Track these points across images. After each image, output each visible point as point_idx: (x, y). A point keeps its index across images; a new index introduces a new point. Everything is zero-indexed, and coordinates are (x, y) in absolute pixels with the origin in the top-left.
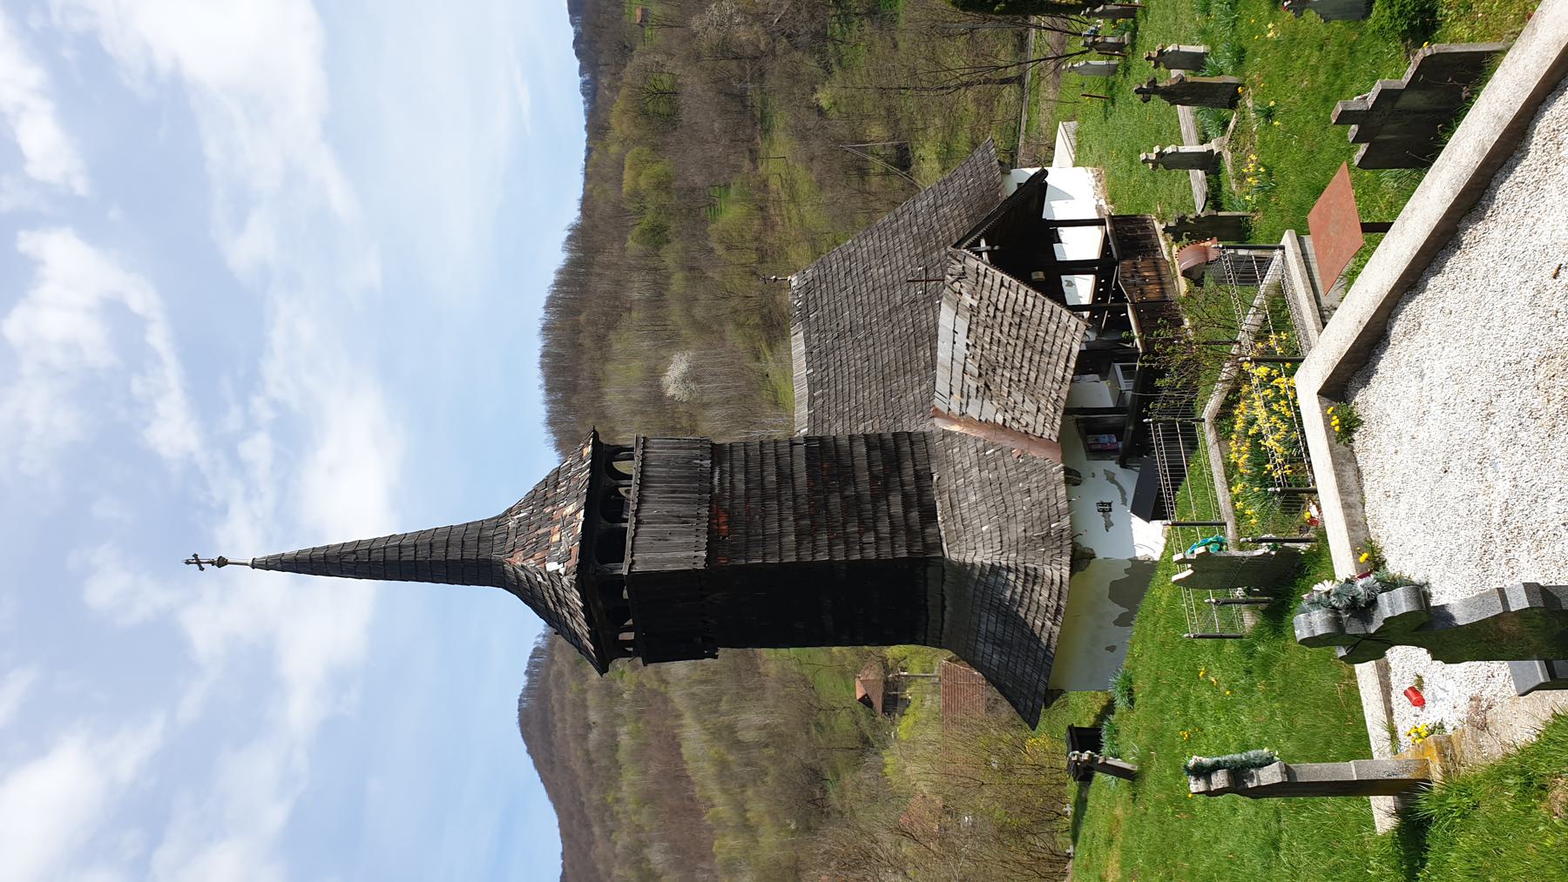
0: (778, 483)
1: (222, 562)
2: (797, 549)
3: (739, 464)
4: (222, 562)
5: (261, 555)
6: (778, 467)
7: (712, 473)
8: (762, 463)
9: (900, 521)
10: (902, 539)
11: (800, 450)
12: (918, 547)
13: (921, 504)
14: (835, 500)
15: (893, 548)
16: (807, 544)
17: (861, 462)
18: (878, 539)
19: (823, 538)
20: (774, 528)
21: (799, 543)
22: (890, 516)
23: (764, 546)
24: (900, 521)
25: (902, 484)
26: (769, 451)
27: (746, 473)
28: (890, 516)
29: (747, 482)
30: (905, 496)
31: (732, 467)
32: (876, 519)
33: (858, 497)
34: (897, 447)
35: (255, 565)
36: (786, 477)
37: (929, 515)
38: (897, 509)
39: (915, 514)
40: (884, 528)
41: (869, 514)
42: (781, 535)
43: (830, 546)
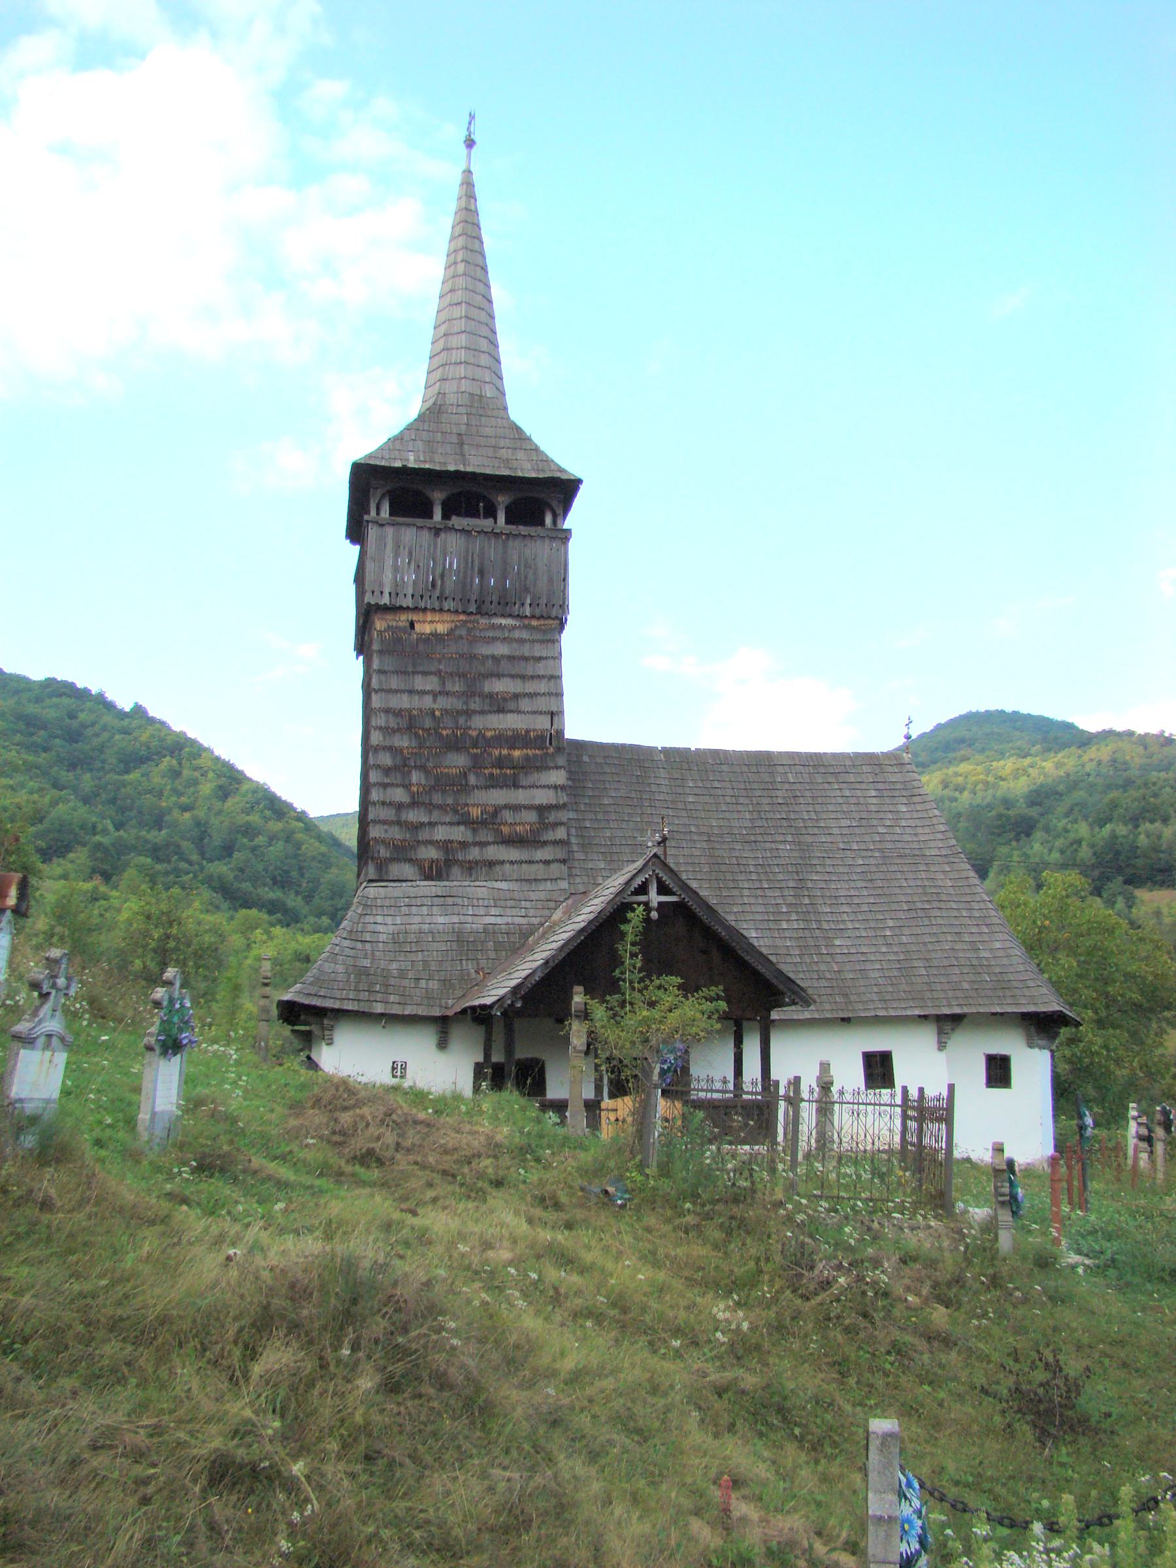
0: (491, 696)
1: (470, 143)
2: (387, 711)
3: (526, 650)
4: (470, 143)
5: (476, 178)
6: (516, 696)
7: (510, 616)
8: (523, 677)
9: (424, 835)
10: (396, 833)
11: (542, 723)
12: (384, 852)
13: (449, 863)
14: (457, 761)
15: (384, 822)
16: (393, 723)
17: (520, 796)
18: (400, 807)
19: (403, 742)
20: (432, 683)
21: (398, 713)
22: (432, 824)
23: (396, 672)
24: (424, 835)
25: (483, 844)
26: (542, 687)
27: (511, 658)
28: (432, 824)
29: (493, 657)
30: (464, 845)
31: (521, 641)
32: (430, 807)
33: (466, 789)
34: (545, 843)
35: (468, 172)
36: (499, 704)
37: (433, 872)
38: (441, 833)
39: (432, 853)
40: (412, 816)
41: (437, 798)
42: (410, 692)
43: (390, 749)
